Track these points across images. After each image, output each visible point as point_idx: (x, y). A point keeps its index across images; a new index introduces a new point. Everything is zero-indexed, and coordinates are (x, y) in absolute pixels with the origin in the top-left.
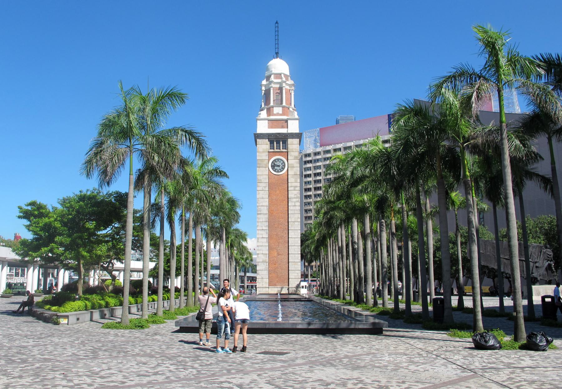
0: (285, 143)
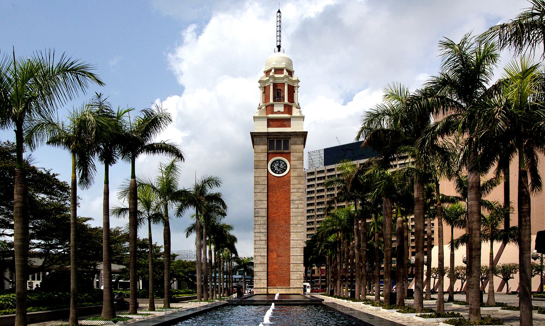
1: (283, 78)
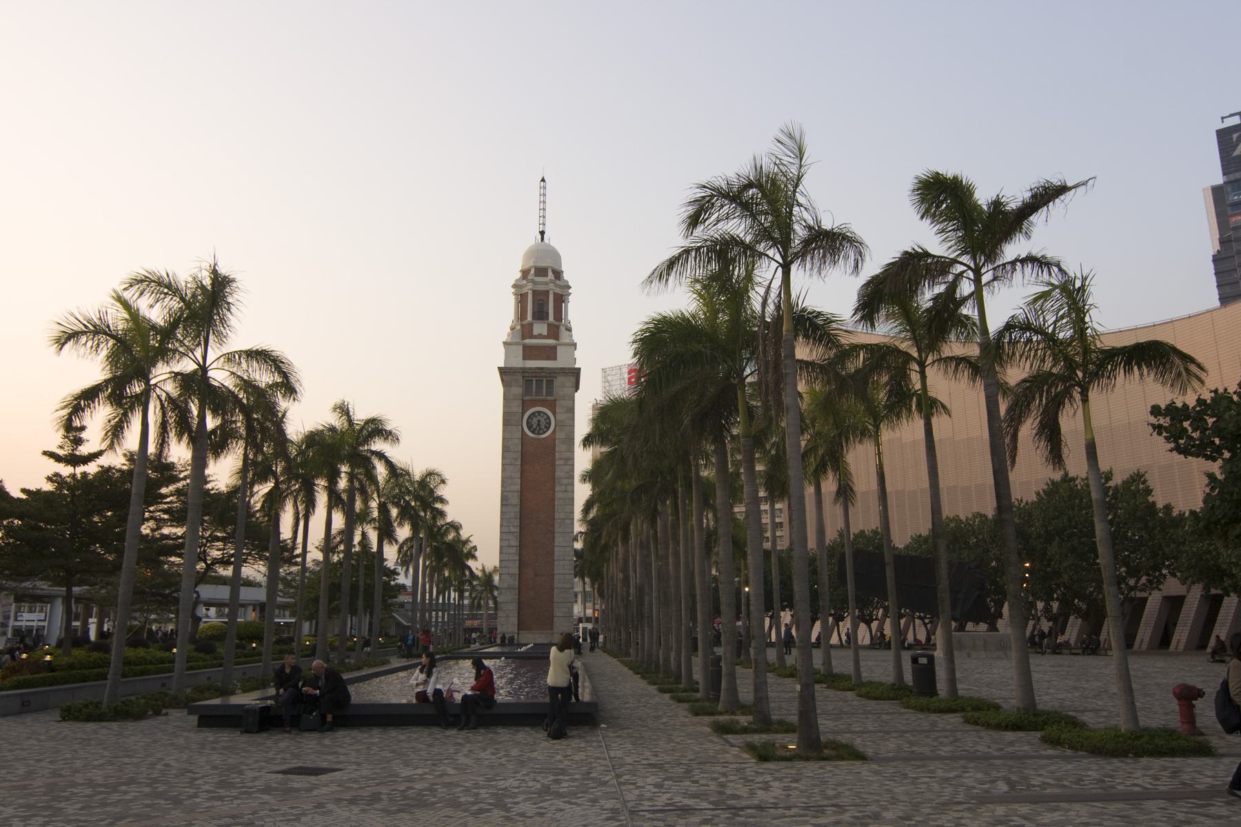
0: (550, 383)
1: (546, 283)
